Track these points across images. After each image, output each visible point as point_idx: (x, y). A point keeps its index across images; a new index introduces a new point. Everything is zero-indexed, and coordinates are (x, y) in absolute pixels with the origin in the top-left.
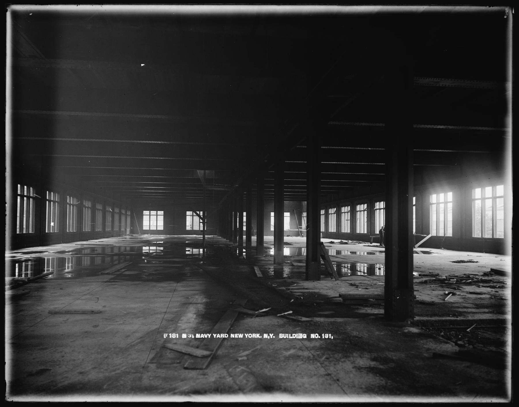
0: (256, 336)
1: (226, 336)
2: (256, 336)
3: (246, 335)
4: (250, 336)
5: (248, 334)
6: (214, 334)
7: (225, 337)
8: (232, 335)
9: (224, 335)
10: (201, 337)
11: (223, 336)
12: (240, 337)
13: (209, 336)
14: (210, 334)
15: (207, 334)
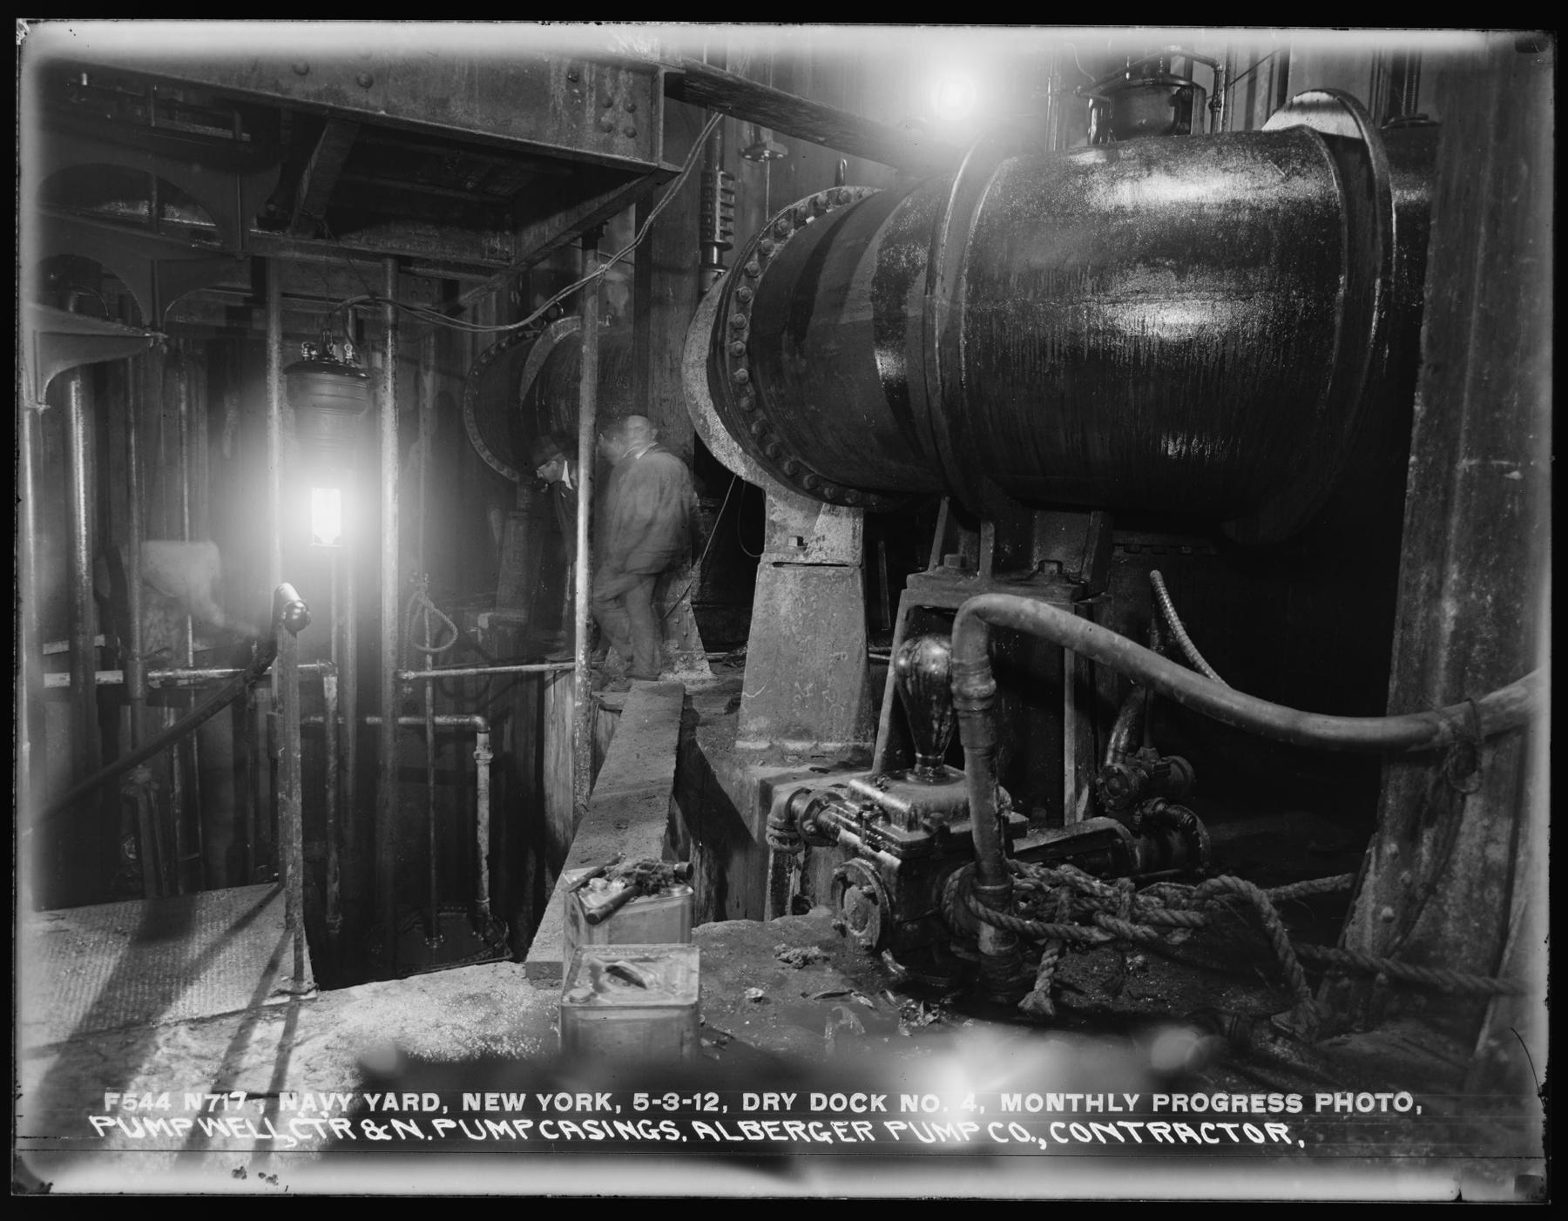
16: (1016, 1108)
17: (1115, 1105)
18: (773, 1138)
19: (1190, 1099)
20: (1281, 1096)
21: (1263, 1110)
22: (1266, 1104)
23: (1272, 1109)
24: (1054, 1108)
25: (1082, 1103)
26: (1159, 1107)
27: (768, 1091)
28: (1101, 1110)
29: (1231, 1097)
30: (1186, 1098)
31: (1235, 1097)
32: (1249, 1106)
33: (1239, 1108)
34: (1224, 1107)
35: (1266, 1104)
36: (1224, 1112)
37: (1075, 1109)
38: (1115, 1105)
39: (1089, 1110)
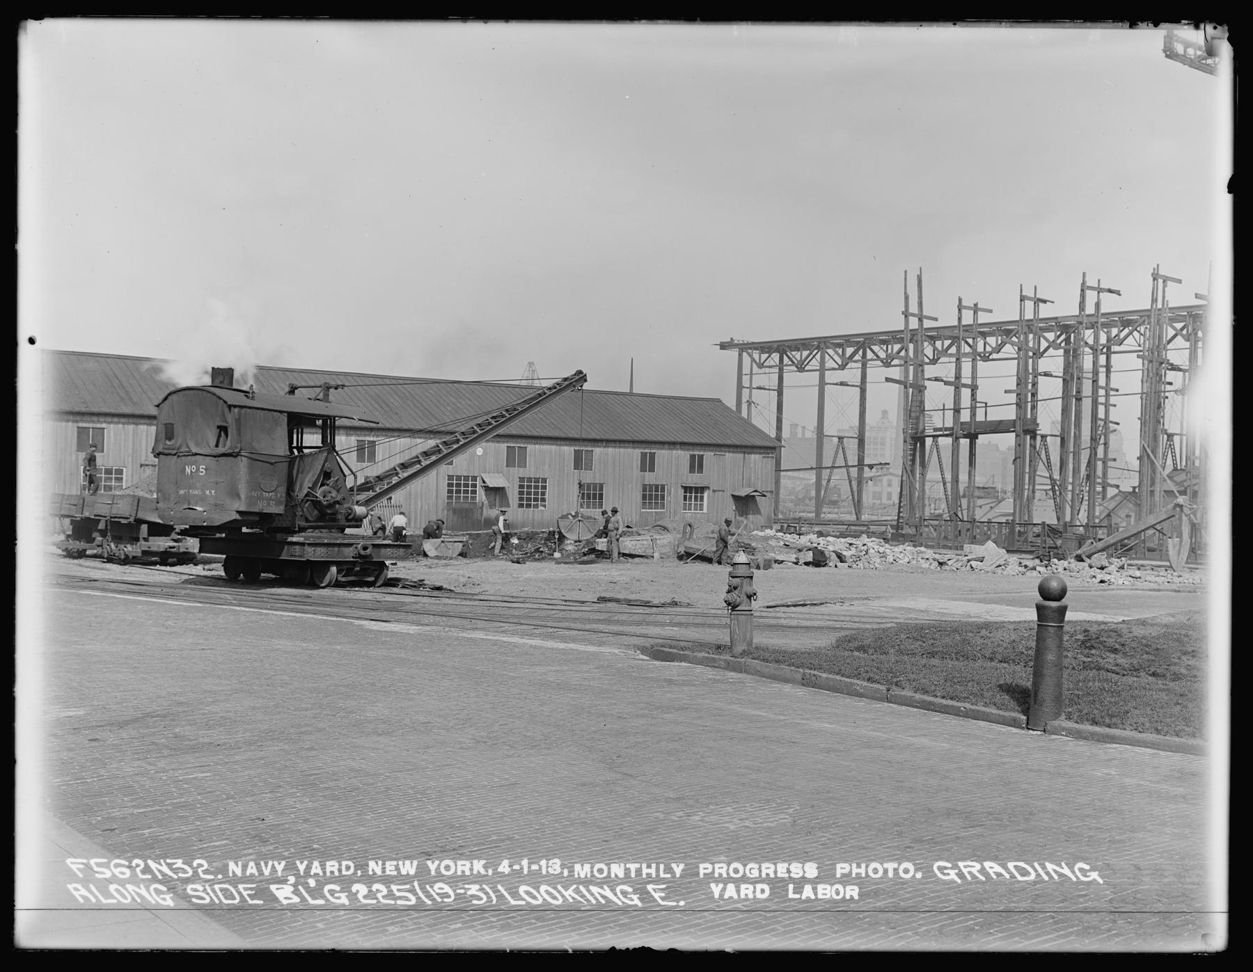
0: (471, 869)
1: (348, 868)
2: (471, 869)
3: (432, 866)
5: (437, 862)
6: (298, 862)
7: (344, 873)
8: (372, 864)
10: (248, 874)
11: (335, 869)
12: (404, 872)
13: (280, 867)
15: (270, 863)
16: (586, 877)
18: (250, 902)
19: (728, 869)
20: (800, 865)
22: (789, 871)
23: (792, 875)
24: (616, 875)
25: (639, 871)
26: (705, 874)
28: (654, 876)
29: (760, 866)
30: (724, 865)
31: (764, 866)
32: (775, 872)
33: (767, 874)
34: (755, 874)
35: (789, 871)
37: (633, 875)
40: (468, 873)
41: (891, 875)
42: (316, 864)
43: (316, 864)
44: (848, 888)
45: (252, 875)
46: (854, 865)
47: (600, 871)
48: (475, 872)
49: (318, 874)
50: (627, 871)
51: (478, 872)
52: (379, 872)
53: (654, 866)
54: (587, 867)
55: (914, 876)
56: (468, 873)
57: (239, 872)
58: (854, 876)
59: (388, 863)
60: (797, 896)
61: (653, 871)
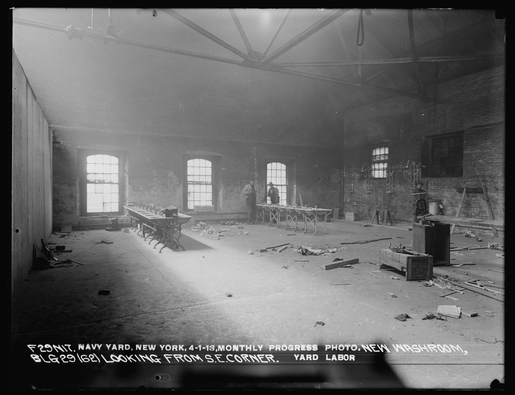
0: (178, 348)
1: (127, 347)
2: (178, 348)
4: (168, 348)
5: (164, 346)
6: (107, 345)
7: (126, 349)
8: (137, 346)
9: (123, 346)
10: (86, 349)
12: (150, 349)
13: (99, 347)
14: (101, 345)
15: (96, 345)
17: (255, 349)
20: (311, 346)
21: (305, 350)
22: (306, 348)
25: (244, 348)
27: (174, 345)
28: (251, 350)
33: (297, 350)
36: (292, 351)
38: (255, 349)
39: (247, 350)
40: (176, 350)
41: (348, 349)
42: (114, 345)
43: (114, 345)
44: (351, 356)
45: (88, 349)
46: (333, 346)
47: (229, 348)
48: (180, 350)
49: (115, 349)
50: (240, 348)
51: (181, 349)
52: (140, 349)
53: (251, 346)
54: (223, 346)
55: (357, 350)
56: (176, 350)
57: (83, 349)
58: (332, 350)
59: (144, 346)
60: (330, 359)
61: (250, 348)
